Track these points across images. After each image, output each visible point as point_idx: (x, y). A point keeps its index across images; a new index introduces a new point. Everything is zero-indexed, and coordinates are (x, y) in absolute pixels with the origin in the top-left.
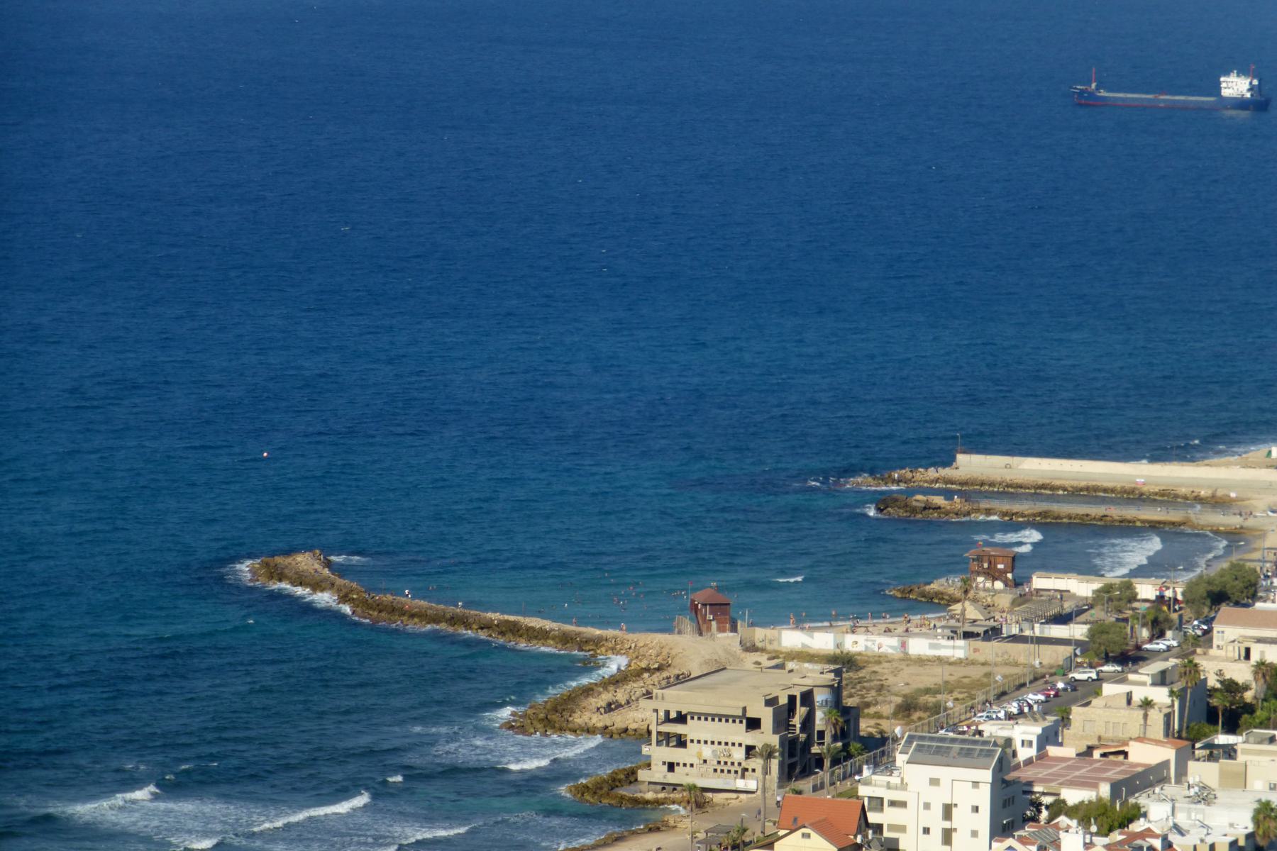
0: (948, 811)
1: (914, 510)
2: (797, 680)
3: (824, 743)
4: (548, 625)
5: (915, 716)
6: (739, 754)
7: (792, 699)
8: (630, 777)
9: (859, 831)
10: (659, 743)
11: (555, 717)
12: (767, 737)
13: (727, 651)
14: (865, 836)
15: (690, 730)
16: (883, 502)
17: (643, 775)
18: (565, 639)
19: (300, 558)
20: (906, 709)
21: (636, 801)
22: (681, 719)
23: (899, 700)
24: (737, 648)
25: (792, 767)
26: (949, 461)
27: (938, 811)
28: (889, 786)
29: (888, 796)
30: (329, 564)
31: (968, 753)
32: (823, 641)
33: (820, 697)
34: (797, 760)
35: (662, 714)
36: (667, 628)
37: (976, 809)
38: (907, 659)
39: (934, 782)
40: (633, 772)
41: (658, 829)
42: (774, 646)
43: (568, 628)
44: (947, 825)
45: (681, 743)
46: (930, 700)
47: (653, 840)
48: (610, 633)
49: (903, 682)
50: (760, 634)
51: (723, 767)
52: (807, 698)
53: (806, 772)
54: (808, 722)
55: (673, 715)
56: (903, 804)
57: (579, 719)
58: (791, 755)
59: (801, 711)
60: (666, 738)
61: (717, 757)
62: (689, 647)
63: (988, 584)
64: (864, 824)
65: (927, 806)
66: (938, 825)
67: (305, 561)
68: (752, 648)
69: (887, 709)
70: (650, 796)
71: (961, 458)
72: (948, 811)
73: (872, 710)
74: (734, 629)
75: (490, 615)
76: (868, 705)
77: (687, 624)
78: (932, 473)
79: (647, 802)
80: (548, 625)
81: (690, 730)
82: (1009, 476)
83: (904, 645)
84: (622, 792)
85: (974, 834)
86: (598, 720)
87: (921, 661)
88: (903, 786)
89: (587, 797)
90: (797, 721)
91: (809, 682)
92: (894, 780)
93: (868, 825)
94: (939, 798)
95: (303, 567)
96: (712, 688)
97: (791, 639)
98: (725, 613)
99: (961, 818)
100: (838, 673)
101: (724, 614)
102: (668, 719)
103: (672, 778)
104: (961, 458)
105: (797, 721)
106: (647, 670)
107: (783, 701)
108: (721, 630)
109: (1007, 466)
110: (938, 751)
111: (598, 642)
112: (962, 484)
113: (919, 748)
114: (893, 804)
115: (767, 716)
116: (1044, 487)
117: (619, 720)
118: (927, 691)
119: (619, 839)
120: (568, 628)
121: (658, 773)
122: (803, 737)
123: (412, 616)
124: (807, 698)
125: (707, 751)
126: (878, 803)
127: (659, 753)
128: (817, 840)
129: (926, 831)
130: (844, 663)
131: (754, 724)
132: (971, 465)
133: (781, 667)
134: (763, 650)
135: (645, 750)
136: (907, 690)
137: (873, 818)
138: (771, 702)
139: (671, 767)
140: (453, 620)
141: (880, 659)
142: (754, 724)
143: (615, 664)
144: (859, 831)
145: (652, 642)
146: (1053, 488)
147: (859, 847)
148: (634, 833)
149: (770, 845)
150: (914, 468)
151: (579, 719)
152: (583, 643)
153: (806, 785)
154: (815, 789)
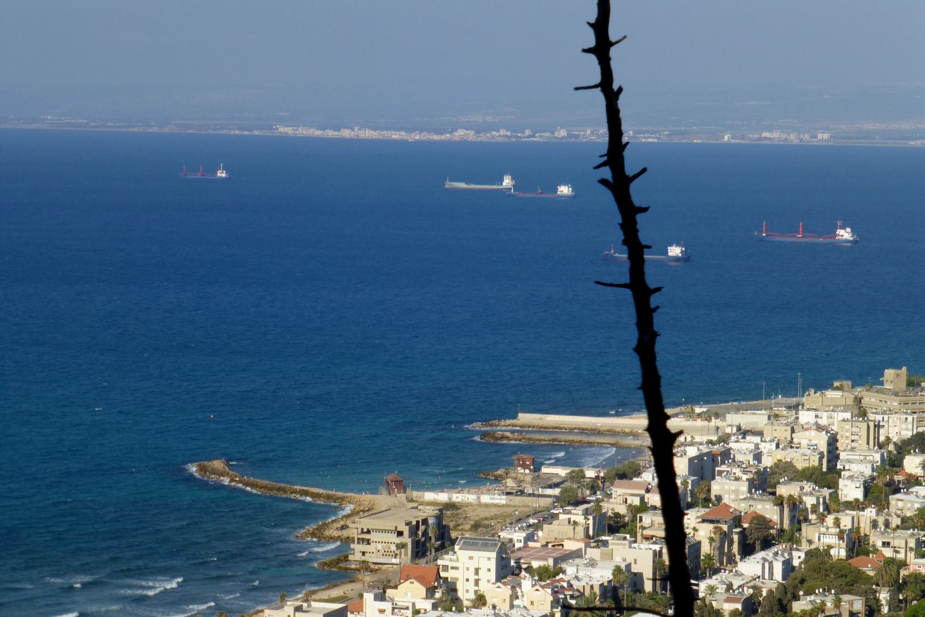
0: (477, 571)
1: (497, 439)
2: (420, 514)
3: (431, 540)
4: (321, 491)
5: (480, 529)
6: (393, 548)
7: (418, 522)
8: (346, 558)
10: (358, 543)
11: (317, 532)
12: (407, 539)
13: (399, 502)
15: (372, 537)
16: (484, 435)
17: (351, 557)
18: (329, 497)
20: (476, 526)
21: (347, 569)
22: (368, 532)
23: (472, 523)
24: (404, 500)
26: (515, 417)
27: (472, 571)
28: (451, 560)
29: (450, 564)
30: (229, 466)
32: (443, 497)
33: (431, 521)
34: (420, 550)
35: (360, 531)
37: (489, 570)
38: (480, 505)
39: (471, 558)
41: (354, 581)
42: (422, 500)
43: (330, 492)
44: (477, 577)
45: (368, 542)
46: (486, 522)
48: (346, 494)
49: (475, 515)
50: (415, 494)
51: (386, 553)
52: (425, 521)
53: (424, 555)
55: (365, 530)
56: (457, 568)
57: (327, 533)
58: (417, 547)
59: (422, 528)
61: (382, 546)
62: (382, 500)
63: (522, 471)
65: (468, 569)
66: (472, 577)
67: (218, 464)
68: (412, 501)
69: (468, 527)
70: (353, 566)
71: (520, 415)
72: (477, 571)
73: (461, 527)
75: (295, 487)
76: (459, 525)
77: (383, 490)
78: (508, 422)
80: (321, 491)
81: (372, 537)
82: (541, 423)
83: (479, 498)
84: (341, 565)
85: (489, 581)
86: (336, 534)
87: (486, 505)
89: (326, 568)
90: (420, 533)
91: (425, 514)
92: (454, 557)
93: (440, 578)
94: (473, 565)
95: (216, 466)
96: (382, 518)
97: (429, 496)
99: (483, 574)
101: (401, 485)
102: (363, 532)
103: (363, 558)
104: (520, 415)
105: (420, 533)
106: (363, 511)
107: (414, 523)
109: (541, 419)
110: (473, 544)
112: (521, 427)
113: (464, 543)
114: (453, 568)
115: (406, 530)
116: (556, 428)
117: (345, 533)
118: (486, 519)
120: (330, 492)
121: (358, 556)
122: (423, 539)
123: (261, 488)
124: (425, 521)
125: (380, 546)
126: (446, 568)
127: (357, 548)
128: (417, 584)
129: (467, 580)
130: (451, 506)
131: (400, 534)
132: (525, 418)
133: (416, 508)
134: (416, 501)
135: (352, 546)
136: (477, 518)
137: (443, 574)
138: (407, 524)
140: (279, 489)
141: (468, 505)
142: (400, 534)
143: (348, 509)
145: (366, 498)
146: (560, 428)
148: (343, 583)
150: (499, 420)
151: (327, 533)
152: (336, 499)
153: (422, 561)
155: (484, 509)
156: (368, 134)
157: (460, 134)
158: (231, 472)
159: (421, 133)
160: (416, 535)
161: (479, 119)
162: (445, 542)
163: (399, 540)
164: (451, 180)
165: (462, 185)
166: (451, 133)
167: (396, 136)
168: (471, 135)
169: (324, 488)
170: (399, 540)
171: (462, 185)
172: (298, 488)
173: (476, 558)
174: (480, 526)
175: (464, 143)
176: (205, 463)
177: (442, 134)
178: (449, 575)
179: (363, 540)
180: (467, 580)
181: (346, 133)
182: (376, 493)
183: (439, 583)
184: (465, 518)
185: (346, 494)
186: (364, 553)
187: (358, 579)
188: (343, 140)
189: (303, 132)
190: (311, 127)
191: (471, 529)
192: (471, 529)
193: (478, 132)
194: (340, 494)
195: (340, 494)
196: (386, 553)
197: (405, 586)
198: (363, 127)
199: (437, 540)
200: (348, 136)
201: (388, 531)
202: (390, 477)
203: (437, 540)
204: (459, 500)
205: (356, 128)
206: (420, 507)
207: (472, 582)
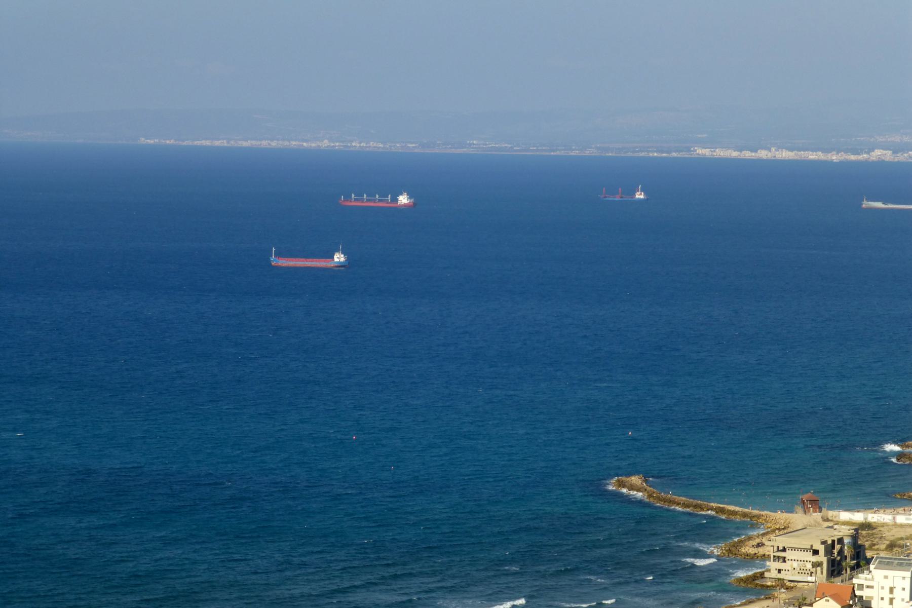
0: (892, 590)
2: (836, 533)
3: (846, 559)
4: (737, 509)
5: (895, 549)
6: (809, 566)
7: (833, 541)
9: (852, 598)
10: (774, 560)
11: (733, 549)
12: (822, 558)
13: (815, 521)
14: (854, 601)
15: (788, 555)
17: (766, 575)
18: (745, 515)
19: (633, 478)
20: (891, 546)
21: (763, 586)
22: (784, 550)
23: (888, 543)
24: (820, 520)
25: (833, 571)
27: (887, 590)
28: (866, 579)
29: (866, 583)
30: (646, 481)
31: (900, 565)
32: (858, 517)
33: (847, 540)
34: (835, 569)
35: (775, 549)
36: (790, 511)
37: (904, 589)
38: (895, 525)
39: (886, 577)
40: (762, 574)
43: (746, 510)
44: (891, 596)
46: (902, 542)
47: (766, 603)
49: (891, 535)
50: (831, 514)
51: (802, 571)
52: (840, 541)
53: (839, 574)
54: (841, 552)
55: (781, 548)
56: (872, 587)
58: (833, 566)
59: (838, 547)
60: (777, 558)
62: (798, 518)
64: (854, 595)
65: (883, 588)
66: (887, 596)
67: (636, 480)
68: (827, 520)
69: (883, 547)
70: (769, 584)
72: (892, 590)
73: (876, 547)
74: (820, 512)
75: (712, 504)
76: (874, 545)
77: (799, 509)
79: (768, 586)
80: (737, 509)
81: (788, 555)
83: (894, 518)
84: (757, 582)
85: (903, 600)
86: (752, 551)
87: (902, 526)
88: (873, 579)
89: (742, 584)
90: (836, 552)
91: (841, 534)
92: (869, 577)
93: (856, 596)
94: (888, 584)
95: (634, 482)
96: (798, 536)
97: (845, 516)
98: (817, 504)
99: (897, 593)
100: (855, 530)
101: (816, 505)
102: (778, 550)
105: (836, 552)
106: (779, 529)
107: (830, 542)
108: (815, 512)
111: (759, 517)
113: (880, 563)
114: (868, 587)
115: (822, 549)
117: (761, 551)
118: (902, 539)
119: (751, 602)
121: (774, 574)
122: (839, 558)
124: (840, 541)
125: (795, 564)
126: (861, 587)
127: (773, 565)
128: (832, 602)
129: (882, 599)
131: (816, 552)
133: (832, 527)
135: (768, 563)
136: (892, 538)
137: (858, 593)
138: (823, 543)
139: (779, 571)
140: (696, 506)
141: (883, 525)
142: (816, 552)
144: (852, 598)
145: (781, 517)
147: (851, 606)
149: (811, 605)
152: (752, 517)
153: (837, 580)
154: (842, 581)
155: (899, 529)
156: (785, 155)
157: (877, 154)
158: (649, 489)
159: (838, 153)
160: (832, 554)
161: (897, 139)
162: (860, 561)
163: (815, 559)
164: (868, 200)
165: (879, 205)
166: (868, 153)
167: (812, 156)
168: (888, 155)
169: (741, 505)
170: (815, 559)
171: (879, 205)
172: (714, 505)
173: (890, 578)
174: (895, 546)
175: (881, 163)
176: (624, 478)
177: (859, 154)
178: (864, 593)
179: (779, 557)
180: (882, 599)
181: (763, 154)
182: (791, 512)
183: (854, 601)
184: (881, 538)
185: (762, 513)
187: (774, 596)
188: (761, 161)
189: (720, 153)
190: (729, 148)
191: (886, 549)
192: (886, 549)
193: (895, 152)
194: (756, 512)
196: (802, 571)
198: (779, 148)
199: (852, 559)
200: (765, 157)
201: (804, 550)
202: (805, 497)
203: (852, 559)
204: (875, 520)
205: (773, 149)
206: (835, 527)
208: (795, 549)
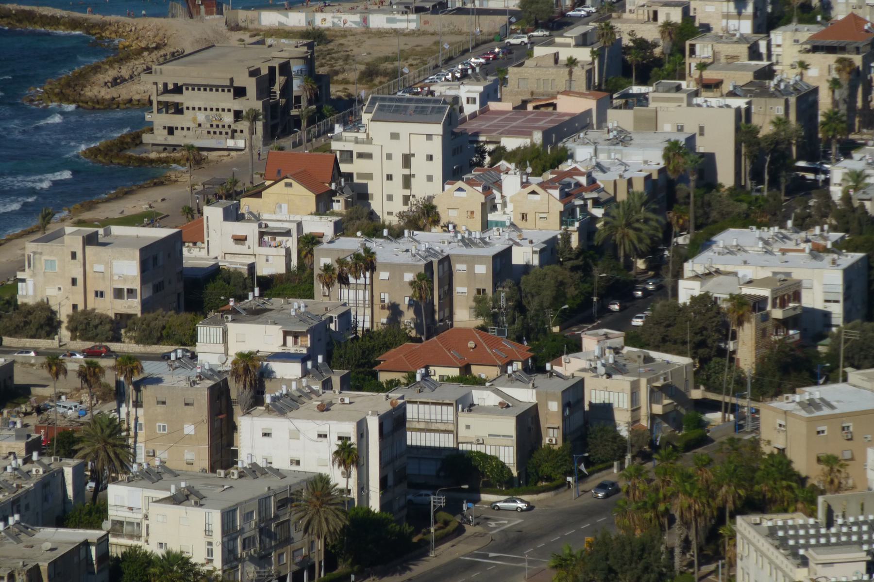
0: (407, 160)
2: (276, 54)
4: (59, 12)
5: (377, 80)
6: (228, 118)
7: (272, 69)
10: (159, 111)
11: (68, 91)
12: (252, 102)
15: (186, 99)
17: (147, 138)
18: (74, 24)
20: (369, 74)
21: (142, 161)
22: (178, 90)
23: (363, 68)
24: (223, 28)
27: (398, 160)
28: (357, 141)
29: (356, 149)
33: (296, 67)
34: (278, 121)
35: (161, 86)
37: (430, 158)
43: (76, 15)
44: (407, 172)
46: (389, 66)
50: (242, 15)
51: (216, 129)
52: (285, 68)
53: (286, 132)
55: (170, 87)
56: (369, 156)
58: (273, 117)
59: (280, 80)
62: (182, 30)
65: (389, 157)
66: (399, 172)
69: (353, 76)
70: (153, 155)
72: (407, 160)
73: (340, 77)
75: (9, 6)
76: (336, 73)
77: (179, 9)
80: (59, 12)
81: (186, 99)
83: (365, 20)
84: (129, 153)
86: (106, 93)
87: (380, 34)
89: (100, 158)
90: (277, 88)
94: (399, 149)
97: (270, 18)
99: (419, 166)
102: (166, 91)
103: (172, 140)
105: (277, 88)
106: (147, 49)
107: (265, 71)
110: (397, 110)
113: (381, 108)
114: (361, 156)
115: (251, 85)
117: (124, 92)
118: (386, 59)
120: (76, 15)
121: (160, 136)
122: (283, 101)
124: (285, 68)
125: (201, 117)
126: (348, 156)
127: (159, 119)
128: (298, 188)
129: (390, 177)
130: (315, 37)
131: (240, 92)
134: (245, 29)
135: (148, 117)
136: (369, 59)
137: (344, 168)
138: (254, 73)
141: (345, 33)
142: (240, 92)
153: (287, 142)
172: (13, 7)
173: (404, 136)
180: (390, 177)
182: (165, 16)
185: (108, 18)
186: (171, 131)
194: (97, 17)
195: (97, 17)
196: (216, 129)
197: (276, 193)
201: (217, 88)
204: (328, 24)
206: (269, 41)
207: (398, 180)
208: (194, 87)
